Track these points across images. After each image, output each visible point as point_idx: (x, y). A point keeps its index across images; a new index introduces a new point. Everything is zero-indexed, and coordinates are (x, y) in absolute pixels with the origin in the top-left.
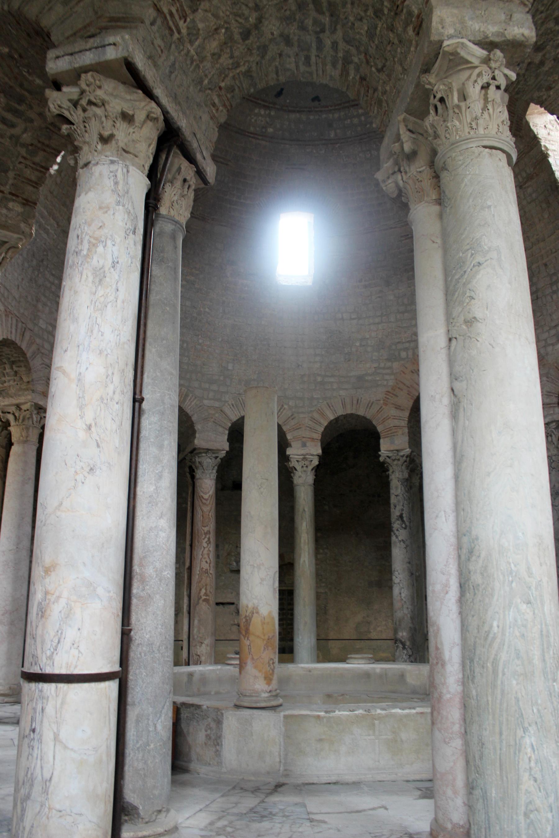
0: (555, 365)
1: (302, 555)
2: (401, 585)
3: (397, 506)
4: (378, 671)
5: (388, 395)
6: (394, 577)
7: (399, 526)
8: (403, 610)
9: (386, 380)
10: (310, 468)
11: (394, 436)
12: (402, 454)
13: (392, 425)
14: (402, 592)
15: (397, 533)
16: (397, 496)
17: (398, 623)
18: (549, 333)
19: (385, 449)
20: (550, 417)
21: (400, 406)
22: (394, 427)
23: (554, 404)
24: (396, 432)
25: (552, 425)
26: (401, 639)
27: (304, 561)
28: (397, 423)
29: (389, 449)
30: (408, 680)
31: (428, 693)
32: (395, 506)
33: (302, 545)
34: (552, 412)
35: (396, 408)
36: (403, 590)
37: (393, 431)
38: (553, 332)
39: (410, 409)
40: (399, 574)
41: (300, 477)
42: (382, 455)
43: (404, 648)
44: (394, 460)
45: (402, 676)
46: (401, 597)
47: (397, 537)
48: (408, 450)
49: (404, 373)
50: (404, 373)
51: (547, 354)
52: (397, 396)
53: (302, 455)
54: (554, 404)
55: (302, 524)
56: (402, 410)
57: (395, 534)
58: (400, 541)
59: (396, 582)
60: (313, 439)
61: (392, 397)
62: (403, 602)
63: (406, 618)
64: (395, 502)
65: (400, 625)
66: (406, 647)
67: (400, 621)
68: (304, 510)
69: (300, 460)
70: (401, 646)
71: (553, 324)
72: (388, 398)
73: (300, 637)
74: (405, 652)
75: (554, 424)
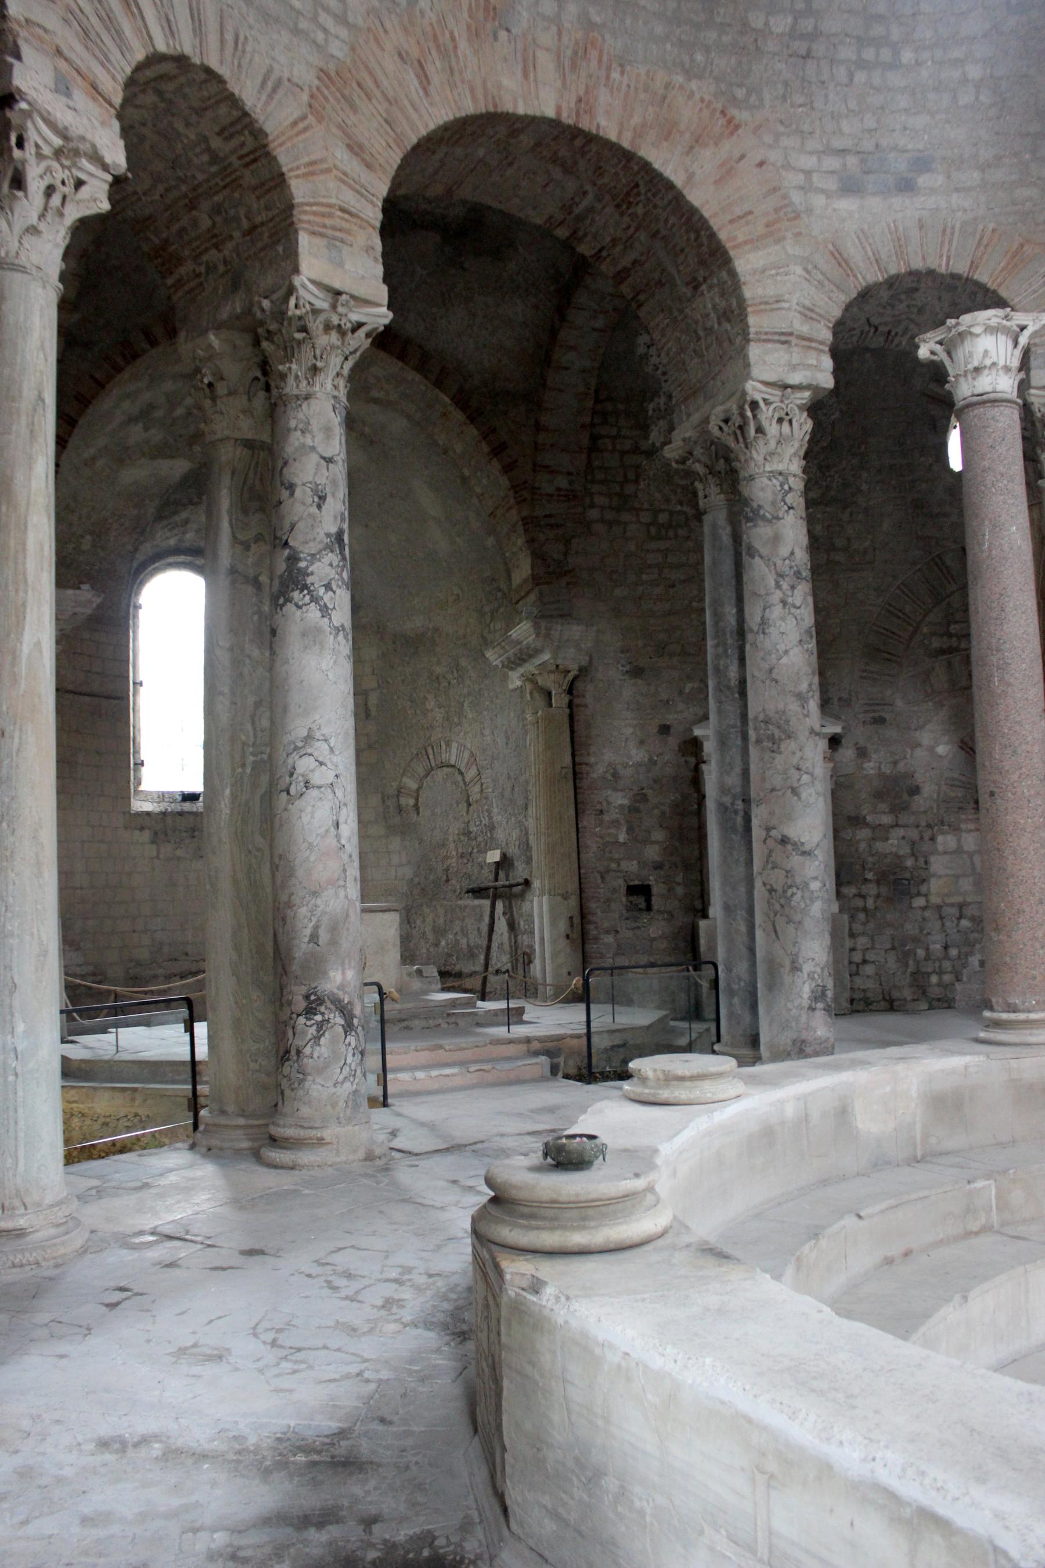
0: (830, 247)
1: (30, 617)
2: (339, 793)
3: (329, 499)
4: (790, 1111)
5: (327, 88)
6: (304, 765)
7: (332, 573)
8: (345, 887)
9: (325, 30)
10: (73, 213)
11: (342, 241)
12: (355, 317)
13: (333, 201)
14: (341, 820)
15: (327, 598)
16: (329, 460)
17: (324, 937)
18: (819, 159)
19: (313, 277)
20: (808, 373)
21: (361, 147)
22: (342, 210)
23: (821, 343)
24: (348, 232)
25: (799, 395)
26: (341, 993)
27: (38, 644)
28: (349, 198)
29: (326, 281)
30: (860, 1126)
31: (919, 1154)
32: (323, 498)
33: (31, 565)
34: (815, 362)
35: (349, 146)
36: (344, 811)
37: (337, 222)
38: (832, 163)
39: (392, 173)
40: (332, 750)
41: (33, 230)
42: (302, 292)
43: (349, 1028)
44: (328, 327)
45: (843, 1112)
46: (338, 837)
47: (325, 611)
48: (384, 310)
49: (376, 40)
50: (376, 40)
51: (809, 211)
52: (354, 108)
53: (63, 133)
54: (821, 343)
55: (30, 460)
56: (368, 166)
57: (315, 599)
58: (337, 630)
59: (316, 779)
60: (94, 87)
61: (339, 102)
62: (345, 857)
63: (352, 914)
64: (321, 480)
65: (334, 942)
66: (355, 1021)
67: (334, 929)
68: (41, 399)
69: (47, 150)
70: (340, 1020)
71: (838, 143)
72: (326, 99)
73: (21, 1027)
74: (351, 1039)
75: (807, 394)
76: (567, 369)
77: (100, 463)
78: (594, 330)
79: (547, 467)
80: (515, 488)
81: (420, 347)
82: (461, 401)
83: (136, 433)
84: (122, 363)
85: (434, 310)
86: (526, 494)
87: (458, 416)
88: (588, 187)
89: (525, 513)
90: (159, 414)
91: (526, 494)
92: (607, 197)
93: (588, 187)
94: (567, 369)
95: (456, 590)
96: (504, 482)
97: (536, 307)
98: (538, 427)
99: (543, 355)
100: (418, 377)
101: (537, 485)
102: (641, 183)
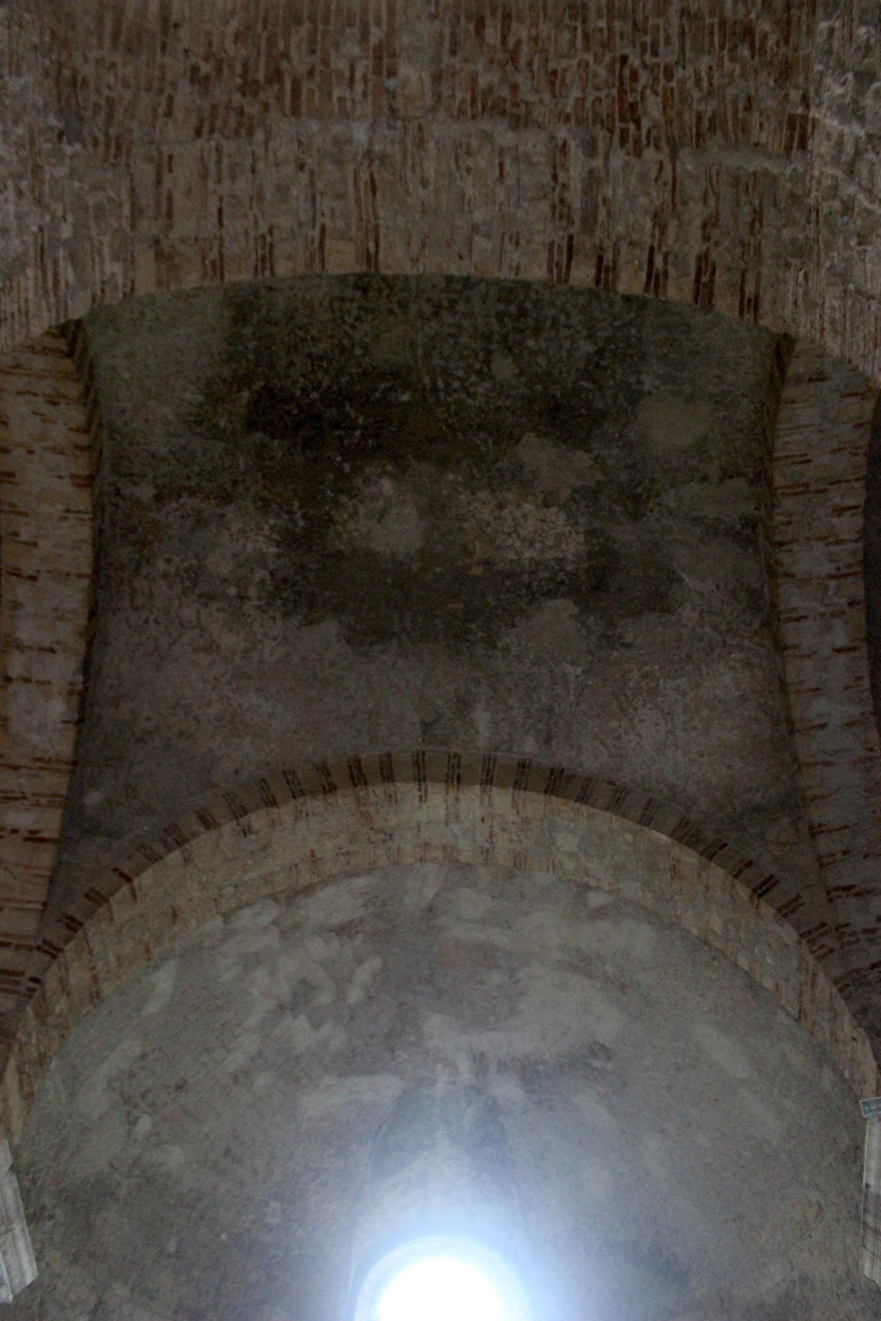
76: (823, 726)
77: (262, 1081)
78: (839, 650)
79: (848, 888)
80: (808, 936)
81: (611, 783)
82: (687, 834)
83: (300, 1031)
84: (159, 848)
85: (613, 724)
86: (829, 941)
87: (690, 858)
88: (562, 133)
89: (836, 972)
90: (324, 998)
91: (829, 941)
92: (601, 134)
93: (562, 133)
94: (823, 726)
95: (815, 1197)
96: (788, 933)
97: (748, 665)
98: (815, 832)
99: (782, 730)
100: (617, 822)
101: (842, 920)
102: (627, 51)
